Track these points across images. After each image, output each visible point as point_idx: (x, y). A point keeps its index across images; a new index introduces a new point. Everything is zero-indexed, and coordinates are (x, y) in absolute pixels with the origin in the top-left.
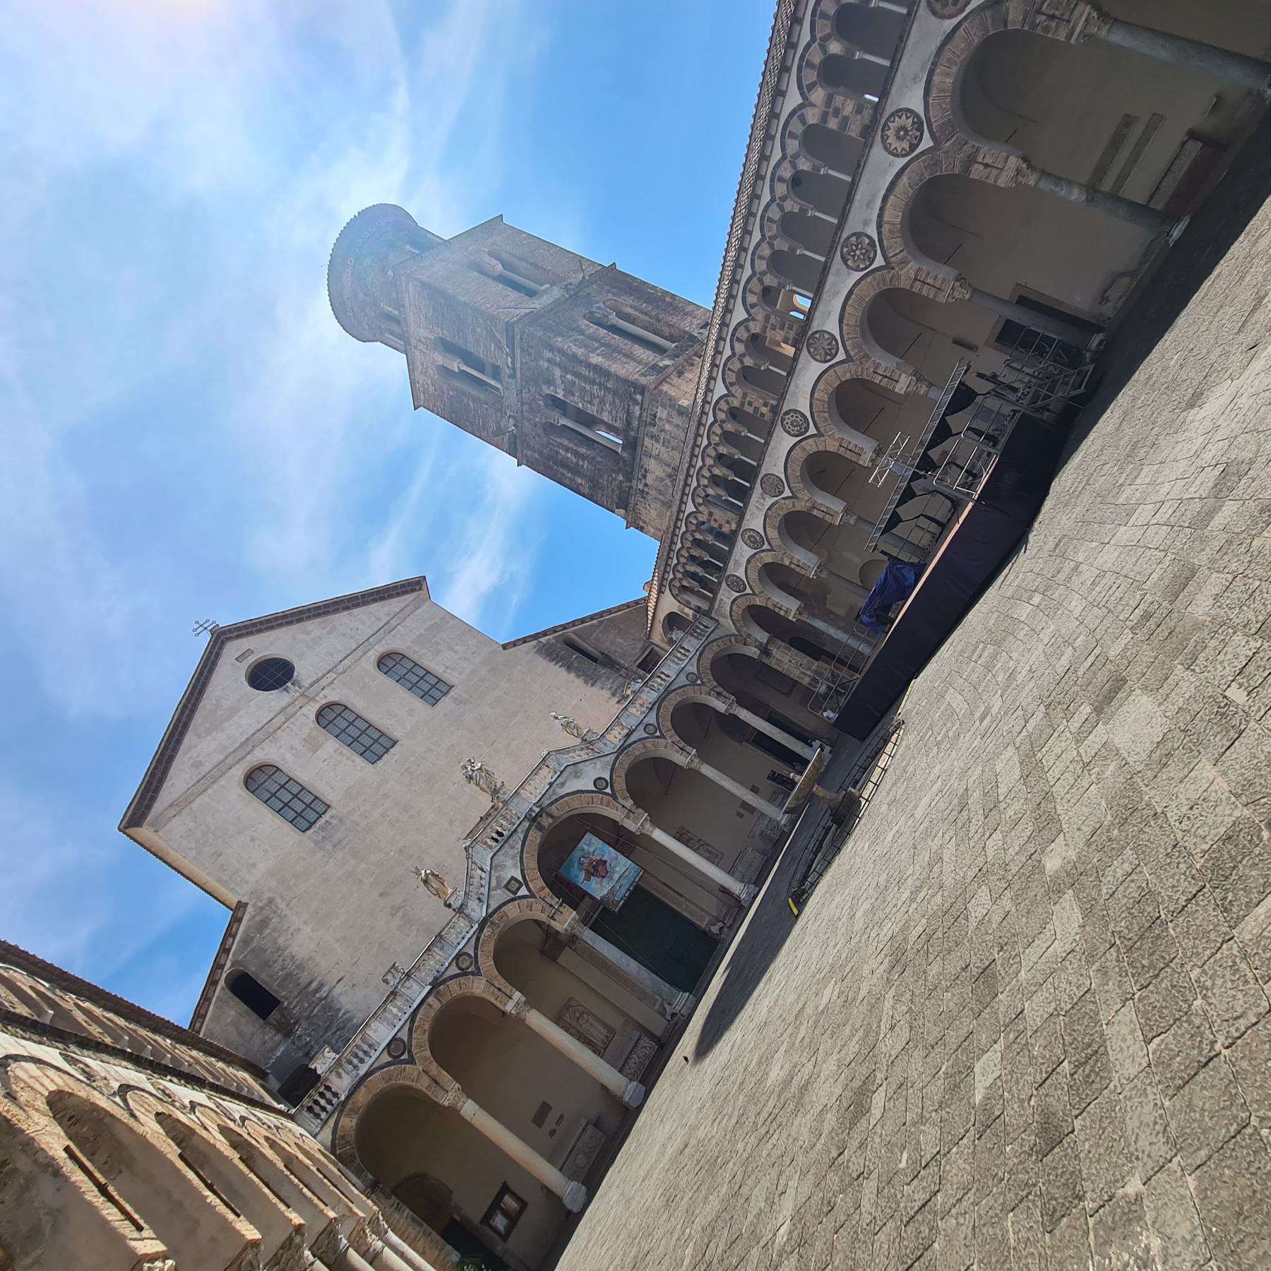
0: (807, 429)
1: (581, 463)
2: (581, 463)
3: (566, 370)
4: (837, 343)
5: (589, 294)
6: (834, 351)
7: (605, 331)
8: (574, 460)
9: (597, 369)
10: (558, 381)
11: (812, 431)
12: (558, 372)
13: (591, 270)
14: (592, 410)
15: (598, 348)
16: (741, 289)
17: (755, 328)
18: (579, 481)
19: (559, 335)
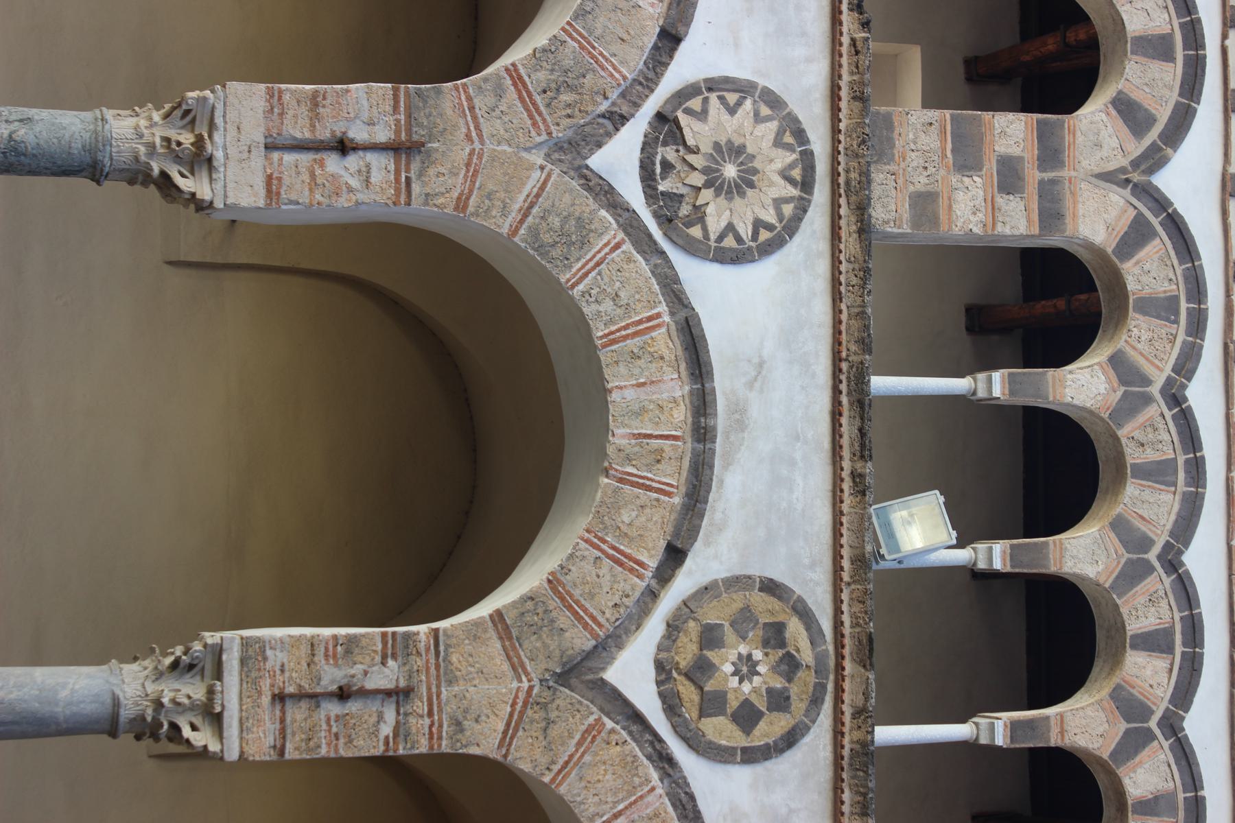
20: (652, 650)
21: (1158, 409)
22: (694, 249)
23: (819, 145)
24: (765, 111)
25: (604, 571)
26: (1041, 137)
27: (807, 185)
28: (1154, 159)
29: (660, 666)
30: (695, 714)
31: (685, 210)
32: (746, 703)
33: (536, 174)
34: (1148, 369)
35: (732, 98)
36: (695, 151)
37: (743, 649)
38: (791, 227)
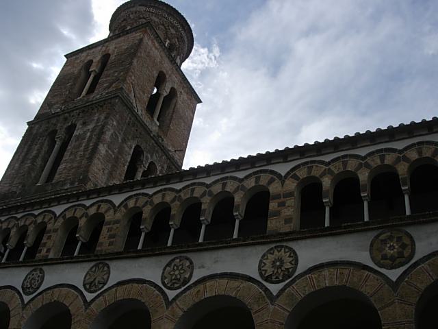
0: (28, 294)
1: (29, 161)
2: (29, 161)
3: (94, 130)
4: (100, 289)
5: (157, 152)
6: (93, 288)
7: (129, 160)
8: (31, 157)
9: (95, 149)
10: (85, 129)
11: (27, 299)
12: (90, 127)
13: (176, 157)
14: (67, 156)
15: (113, 152)
16: (138, 192)
17: (109, 217)
18: (17, 165)
19: (118, 122)
20: (388, 271)
21: (331, 167)
22: (295, 269)
23: (273, 245)
24: (266, 257)
25: (368, 284)
26: (274, 199)
27: (282, 246)
28: (279, 176)
29: (392, 268)
30: (404, 259)
31: (286, 273)
32: (400, 247)
33: (276, 307)
34: (323, 170)
35: (263, 265)
36: (274, 271)
37: (387, 249)
38: (290, 249)
